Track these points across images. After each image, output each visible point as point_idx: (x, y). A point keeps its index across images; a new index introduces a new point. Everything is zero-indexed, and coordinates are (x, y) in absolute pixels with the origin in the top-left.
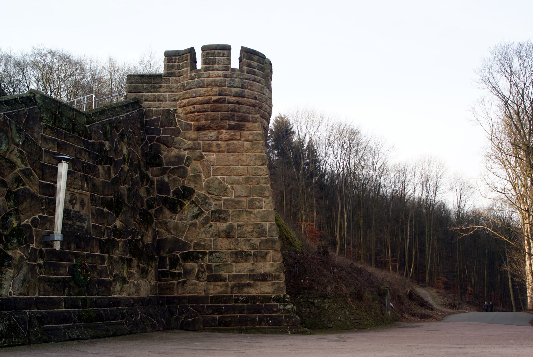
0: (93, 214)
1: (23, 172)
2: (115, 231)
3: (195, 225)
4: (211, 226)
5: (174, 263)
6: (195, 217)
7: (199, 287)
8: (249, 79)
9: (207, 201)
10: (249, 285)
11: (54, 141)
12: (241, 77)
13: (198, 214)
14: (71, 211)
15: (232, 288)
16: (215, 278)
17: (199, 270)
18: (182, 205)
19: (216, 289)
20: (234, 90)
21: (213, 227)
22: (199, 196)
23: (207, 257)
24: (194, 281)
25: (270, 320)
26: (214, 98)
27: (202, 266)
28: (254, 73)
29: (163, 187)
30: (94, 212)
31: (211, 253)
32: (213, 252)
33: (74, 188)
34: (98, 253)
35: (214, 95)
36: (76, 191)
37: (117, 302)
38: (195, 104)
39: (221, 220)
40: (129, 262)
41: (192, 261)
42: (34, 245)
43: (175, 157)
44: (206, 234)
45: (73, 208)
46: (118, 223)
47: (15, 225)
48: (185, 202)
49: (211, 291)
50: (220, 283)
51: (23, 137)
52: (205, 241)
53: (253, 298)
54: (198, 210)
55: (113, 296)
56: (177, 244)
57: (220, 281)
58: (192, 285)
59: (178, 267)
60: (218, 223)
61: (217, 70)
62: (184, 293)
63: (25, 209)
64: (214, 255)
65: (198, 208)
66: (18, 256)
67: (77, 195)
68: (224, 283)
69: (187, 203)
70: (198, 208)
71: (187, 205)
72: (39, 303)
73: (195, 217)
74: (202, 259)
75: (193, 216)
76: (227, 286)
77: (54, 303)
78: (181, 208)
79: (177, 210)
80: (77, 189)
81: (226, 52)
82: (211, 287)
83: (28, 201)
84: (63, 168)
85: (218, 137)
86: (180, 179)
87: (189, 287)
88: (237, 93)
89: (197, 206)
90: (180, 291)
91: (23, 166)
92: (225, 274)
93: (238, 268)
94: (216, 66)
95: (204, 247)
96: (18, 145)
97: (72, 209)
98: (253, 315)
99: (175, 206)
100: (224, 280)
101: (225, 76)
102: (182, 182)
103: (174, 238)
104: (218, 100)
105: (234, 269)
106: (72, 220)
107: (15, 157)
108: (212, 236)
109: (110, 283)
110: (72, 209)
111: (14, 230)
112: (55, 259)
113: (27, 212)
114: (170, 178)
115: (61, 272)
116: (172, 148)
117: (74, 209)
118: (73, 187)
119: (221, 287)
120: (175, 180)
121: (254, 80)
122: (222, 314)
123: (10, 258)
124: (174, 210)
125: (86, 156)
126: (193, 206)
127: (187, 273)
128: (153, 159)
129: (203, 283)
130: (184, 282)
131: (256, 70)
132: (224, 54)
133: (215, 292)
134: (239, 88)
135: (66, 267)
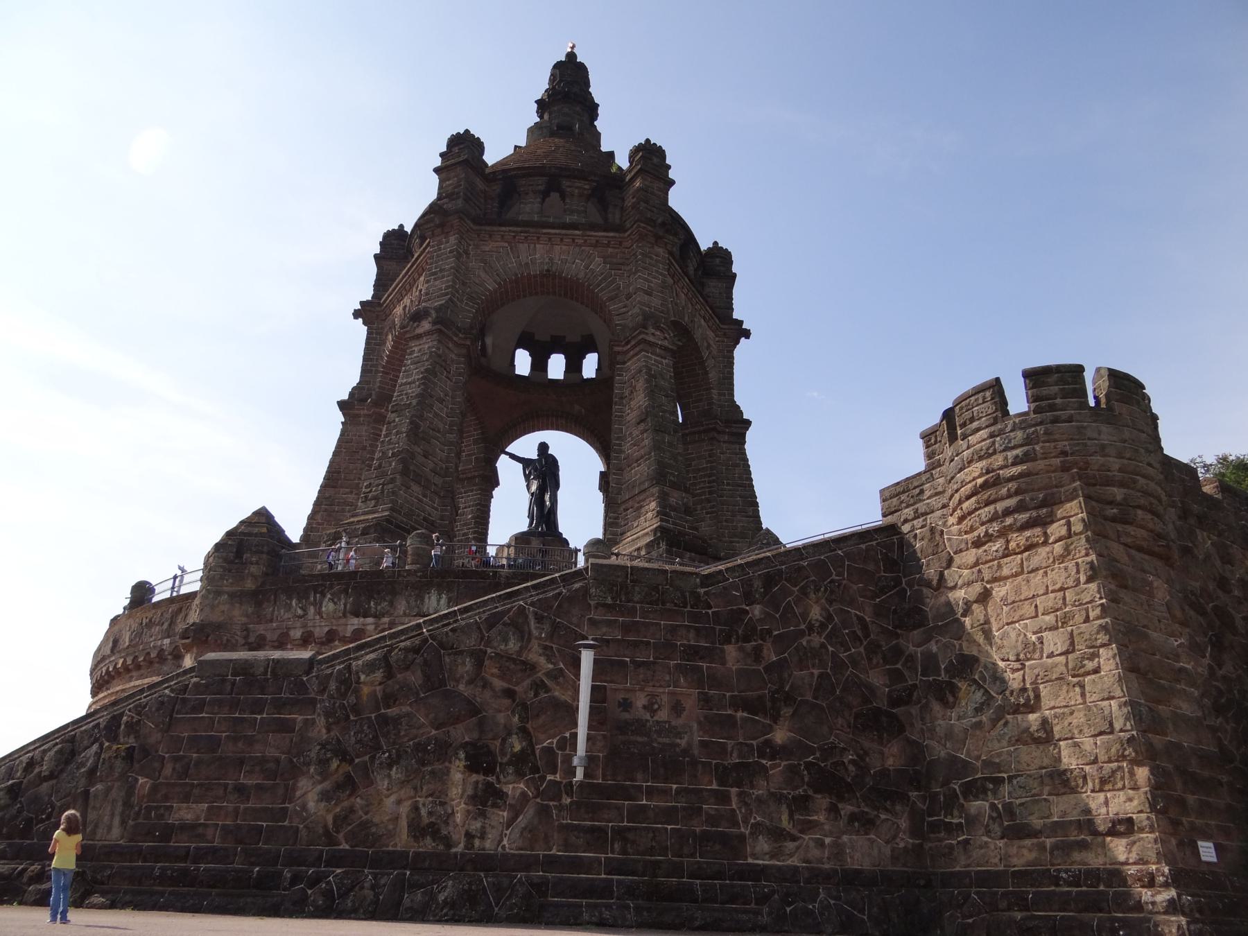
0: (699, 723)
1: (548, 674)
2: (773, 751)
3: (979, 725)
4: (1006, 724)
5: (951, 802)
6: (978, 710)
7: (993, 852)
8: (1041, 423)
10: (1083, 846)
11: (610, 623)
13: (982, 704)
14: (647, 721)
15: (1051, 853)
16: (1018, 832)
17: (991, 817)
18: (954, 689)
19: (1023, 855)
20: (1011, 454)
21: (1010, 725)
22: (986, 667)
23: (1006, 789)
24: (985, 839)
25: (1120, 928)
26: (980, 481)
27: (993, 807)
28: (1052, 408)
29: (930, 663)
31: (1010, 778)
32: (1016, 777)
34: (715, 787)
35: (979, 477)
36: (661, 690)
37: (758, 873)
38: (960, 502)
40: (800, 804)
41: (977, 798)
44: (999, 741)
46: (780, 736)
47: (517, 748)
49: (1015, 861)
50: (1028, 842)
51: (547, 627)
52: (999, 755)
53: (1093, 876)
55: (750, 861)
56: (958, 767)
57: (1029, 836)
58: (981, 847)
59: (956, 813)
60: (1019, 717)
61: (978, 430)
62: (969, 866)
64: (1015, 782)
65: (982, 691)
66: (518, 793)
68: (1035, 841)
69: (963, 685)
70: (982, 691)
72: (551, 863)
73: (978, 710)
74: (995, 793)
76: (1042, 847)
77: (577, 865)
78: (954, 696)
82: (1014, 850)
84: (587, 659)
85: (1007, 548)
87: (976, 854)
88: (1017, 456)
89: (980, 687)
90: (963, 860)
91: (551, 666)
92: (1037, 822)
93: (1062, 807)
94: (975, 425)
95: (998, 767)
96: (540, 638)
98: (1087, 916)
99: (946, 694)
100: (1035, 834)
101: (992, 436)
103: (948, 754)
104: (986, 482)
105: (1055, 810)
107: (535, 655)
108: (1010, 743)
109: (742, 838)
111: (514, 755)
117: (655, 718)
119: (1030, 851)
120: (946, 646)
121: (1056, 420)
122: (1028, 910)
123: (500, 795)
124: (946, 704)
125: (692, 635)
126: (973, 688)
127: (972, 821)
129: (1001, 843)
130: (967, 842)
131: (1058, 401)
132: (984, 398)
133: (1022, 861)
134: (1021, 446)
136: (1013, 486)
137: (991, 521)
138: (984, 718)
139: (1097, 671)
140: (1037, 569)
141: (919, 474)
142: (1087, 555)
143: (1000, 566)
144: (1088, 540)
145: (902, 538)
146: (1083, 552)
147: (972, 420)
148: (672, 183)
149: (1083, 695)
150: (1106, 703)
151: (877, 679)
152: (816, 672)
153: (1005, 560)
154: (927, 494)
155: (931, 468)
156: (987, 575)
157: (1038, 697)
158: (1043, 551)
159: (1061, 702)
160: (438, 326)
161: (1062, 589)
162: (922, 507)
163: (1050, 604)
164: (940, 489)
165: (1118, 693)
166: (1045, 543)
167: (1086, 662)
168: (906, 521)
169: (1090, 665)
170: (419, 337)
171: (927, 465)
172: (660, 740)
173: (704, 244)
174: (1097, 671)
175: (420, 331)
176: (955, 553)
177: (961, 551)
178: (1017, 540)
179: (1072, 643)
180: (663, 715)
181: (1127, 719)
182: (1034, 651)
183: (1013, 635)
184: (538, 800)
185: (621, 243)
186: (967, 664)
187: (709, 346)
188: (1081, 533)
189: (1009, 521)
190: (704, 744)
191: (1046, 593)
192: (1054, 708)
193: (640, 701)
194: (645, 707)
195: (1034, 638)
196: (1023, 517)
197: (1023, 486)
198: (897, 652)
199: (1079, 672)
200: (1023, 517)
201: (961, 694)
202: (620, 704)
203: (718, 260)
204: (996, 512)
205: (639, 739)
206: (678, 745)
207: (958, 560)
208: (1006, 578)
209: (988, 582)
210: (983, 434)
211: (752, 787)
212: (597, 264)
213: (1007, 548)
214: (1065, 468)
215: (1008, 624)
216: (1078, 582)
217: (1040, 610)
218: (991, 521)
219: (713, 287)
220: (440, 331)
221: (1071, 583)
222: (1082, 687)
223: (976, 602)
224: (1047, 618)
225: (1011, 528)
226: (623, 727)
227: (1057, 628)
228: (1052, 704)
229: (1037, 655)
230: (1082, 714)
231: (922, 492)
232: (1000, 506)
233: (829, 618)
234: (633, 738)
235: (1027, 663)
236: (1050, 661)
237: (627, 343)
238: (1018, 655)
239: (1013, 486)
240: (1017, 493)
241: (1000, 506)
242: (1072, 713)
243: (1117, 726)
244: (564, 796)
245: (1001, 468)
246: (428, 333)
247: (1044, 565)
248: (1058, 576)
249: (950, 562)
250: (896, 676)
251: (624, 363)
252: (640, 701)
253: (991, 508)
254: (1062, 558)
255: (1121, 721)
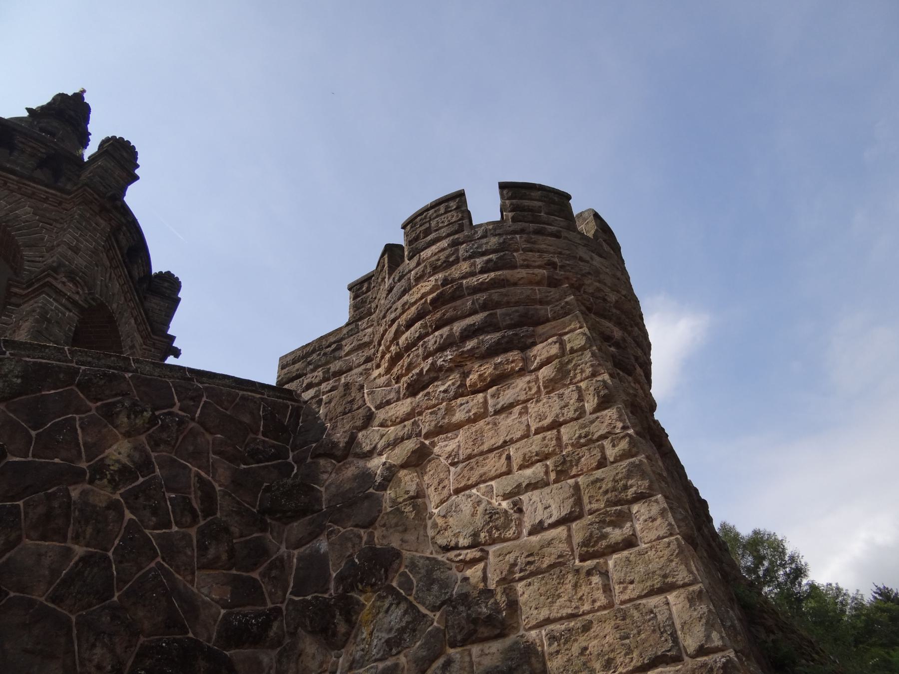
4: (449, 663)
6: (394, 644)
9: (437, 574)
12: (498, 231)
13: (402, 631)
18: (349, 610)
20: (480, 262)
21: (455, 667)
22: (413, 566)
29: (314, 568)
38: (398, 334)
39: (484, 631)
43: (355, 478)
48: (362, 599)
54: (406, 612)
60: (475, 650)
65: (403, 606)
69: (367, 600)
70: (403, 606)
71: (368, 605)
75: (388, 642)
79: (334, 634)
81: (453, 205)
85: (463, 385)
86: (362, 531)
102: (365, 538)
114: (333, 538)
116: (350, 459)
121: (538, 232)
128: (295, 503)
132: (447, 207)
136: (482, 297)
137: (441, 349)
138: (402, 659)
139: (630, 543)
140: (511, 406)
141: (341, 329)
142: (594, 375)
143: (449, 411)
144: (593, 355)
145: (300, 408)
146: (588, 371)
147: (427, 232)
148: (136, 178)
149: (607, 589)
150: (653, 601)
151: (208, 589)
152: (80, 550)
153: (459, 401)
154: (347, 349)
155: (354, 321)
156: (426, 423)
157: (513, 605)
158: (521, 383)
159: (561, 608)
161: (556, 425)
162: (335, 366)
163: (535, 448)
164: (366, 339)
165: (682, 576)
166: (522, 372)
167: (609, 529)
168: (310, 386)
169: (616, 535)
171: (352, 317)
173: (157, 267)
174: (630, 543)
176: (378, 407)
177: (388, 403)
178: (479, 371)
179: (578, 502)
181: (710, 626)
182: (506, 526)
183: (466, 507)
185: (60, 203)
186: (378, 565)
187: (132, 347)
188: (583, 349)
189: (470, 345)
191: (526, 436)
192: (548, 621)
195: (505, 505)
196: (491, 338)
197: (495, 297)
198: (259, 552)
199: (595, 550)
200: (491, 338)
201: (364, 615)
203: (166, 284)
204: (451, 335)
207: (381, 415)
208: (459, 426)
209: (427, 436)
210: (444, 243)
212: (26, 211)
213: (463, 385)
214: (553, 283)
215: (457, 491)
216: (581, 413)
217: (516, 461)
218: (441, 349)
219: (154, 303)
221: (571, 414)
222: (605, 574)
223: (403, 466)
224: (528, 472)
225: (472, 355)
227: (547, 484)
228: (544, 613)
229: (510, 533)
230: (608, 628)
231: (339, 348)
232: (458, 327)
233: (145, 466)
235: (492, 550)
236: (534, 539)
237: (28, 287)
238: (475, 535)
239: (482, 297)
240: (484, 307)
241: (458, 327)
242: (586, 628)
243: (690, 643)
245: (464, 277)
247: (523, 397)
248: (548, 408)
249: (369, 418)
250: (246, 591)
251: (18, 306)
253: (445, 331)
254: (552, 385)
255: (699, 630)
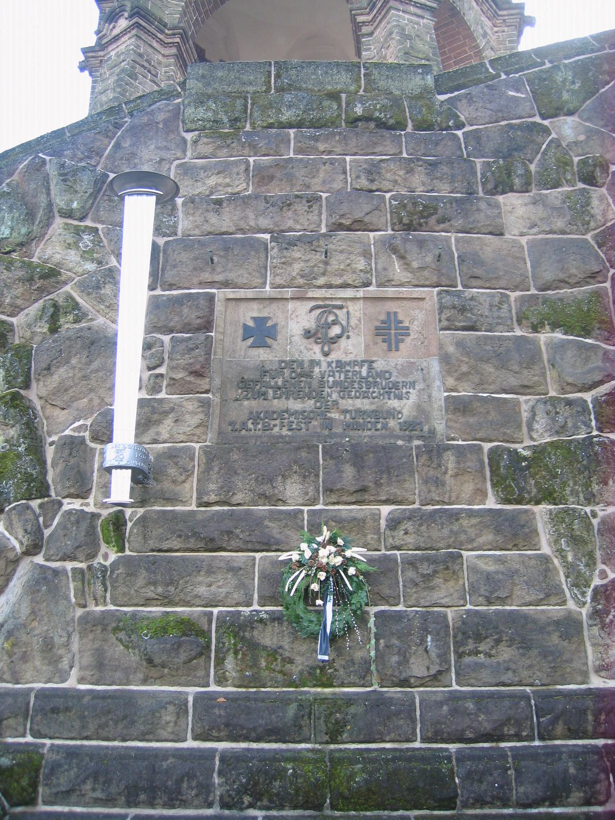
0: (445, 359)
14: (314, 363)
30: (451, 349)
33: (329, 286)
34: (491, 503)
36: (349, 293)
42: (91, 500)
45: (326, 355)
63: (61, 389)
67: (356, 310)
77: (119, 712)
80: (345, 286)
83: (74, 361)
91: (90, 267)
97: (318, 356)
106: (319, 396)
110: (318, 356)
112: (176, 543)
113: (75, 399)
115: (202, 590)
117: (333, 357)
118: (321, 281)
135: (233, 570)
160: (136, 19)
170: (116, 38)
172: (347, 404)
175: (116, 32)
180: (352, 348)
184: (39, 559)
187: (485, 35)
190: (458, 407)
193: (296, 319)
194: (308, 334)
202: (247, 333)
205: (295, 405)
206: (393, 413)
211: (591, 499)
220: (138, 25)
226: (251, 384)
234: (278, 404)
237: (371, 10)
244: (104, 548)
246: (124, 32)
251: (371, 34)
252: (296, 319)
